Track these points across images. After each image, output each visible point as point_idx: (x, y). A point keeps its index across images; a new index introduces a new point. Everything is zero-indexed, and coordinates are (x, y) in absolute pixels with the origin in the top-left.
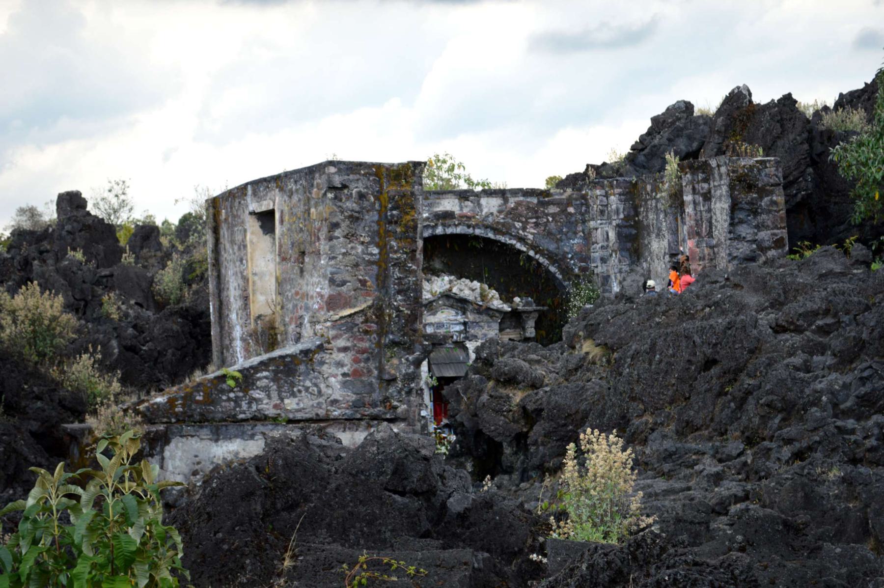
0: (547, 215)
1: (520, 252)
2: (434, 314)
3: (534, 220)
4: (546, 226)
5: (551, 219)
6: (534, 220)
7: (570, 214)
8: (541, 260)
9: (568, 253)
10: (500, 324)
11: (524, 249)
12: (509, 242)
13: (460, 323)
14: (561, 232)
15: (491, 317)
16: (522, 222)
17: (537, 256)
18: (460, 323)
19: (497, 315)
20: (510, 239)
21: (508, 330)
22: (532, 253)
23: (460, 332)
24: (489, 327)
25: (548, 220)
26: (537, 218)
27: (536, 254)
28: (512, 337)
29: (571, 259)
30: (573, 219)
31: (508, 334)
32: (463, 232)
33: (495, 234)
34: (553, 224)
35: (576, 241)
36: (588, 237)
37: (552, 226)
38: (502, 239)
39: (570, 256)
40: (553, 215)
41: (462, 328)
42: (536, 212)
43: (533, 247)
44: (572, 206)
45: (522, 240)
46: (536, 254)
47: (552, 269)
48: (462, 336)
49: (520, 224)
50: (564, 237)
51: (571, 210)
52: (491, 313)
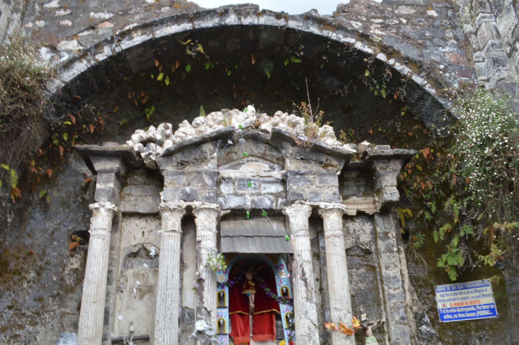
0: (398, 16)
1: (362, 54)
2: (237, 166)
3: (380, 21)
4: (399, 28)
5: (404, 21)
6: (380, 21)
7: (431, 17)
8: (398, 66)
9: (439, 63)
10: (340, 177)
11: (370, 51)
12: (343, 39)
13: (276, 181)
14: (422, 36)
15: (326, 166)
16: (361, 21)
17: (391, 62)
18: (276, 181)
19: (335, 163)
20: (345, 36)
21: (354, 198)
22: (381, 57)
23: (277, 195)
24: (321, 182)
25: (401, 22)
26: (385, 18)
27: (389, 58)
28: (362, 207)
29: (445, 70)
30: (437, 23)
31: (354, 203)
32: (269, 23)
33: (321, 30)
34: (408, 27)
35: (447, 49)
36: (464, 43)
37: (408, 29)
38: (333, 36)
39: (442, 67)
40: (408, 17)
41: (280, 188)
42: (382, 12)
43: (384, 49)
44: (433, 9)
45: (364, 37)
46: (389, 58)
47: (418, 80)
48: (280, 200)
49: (360, 24)
50: (428, 43)
51: (432, 13)
52: (323, 158)
